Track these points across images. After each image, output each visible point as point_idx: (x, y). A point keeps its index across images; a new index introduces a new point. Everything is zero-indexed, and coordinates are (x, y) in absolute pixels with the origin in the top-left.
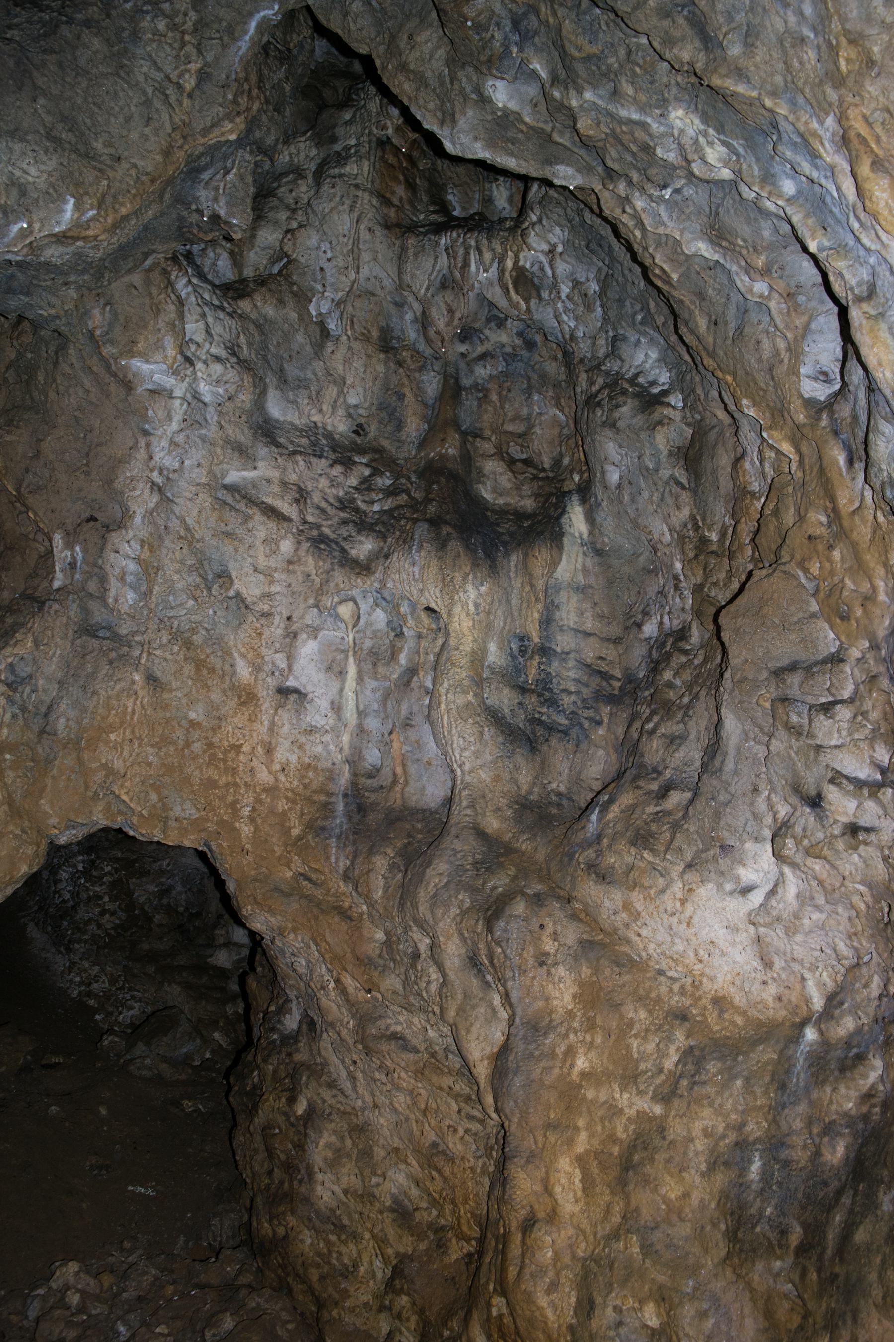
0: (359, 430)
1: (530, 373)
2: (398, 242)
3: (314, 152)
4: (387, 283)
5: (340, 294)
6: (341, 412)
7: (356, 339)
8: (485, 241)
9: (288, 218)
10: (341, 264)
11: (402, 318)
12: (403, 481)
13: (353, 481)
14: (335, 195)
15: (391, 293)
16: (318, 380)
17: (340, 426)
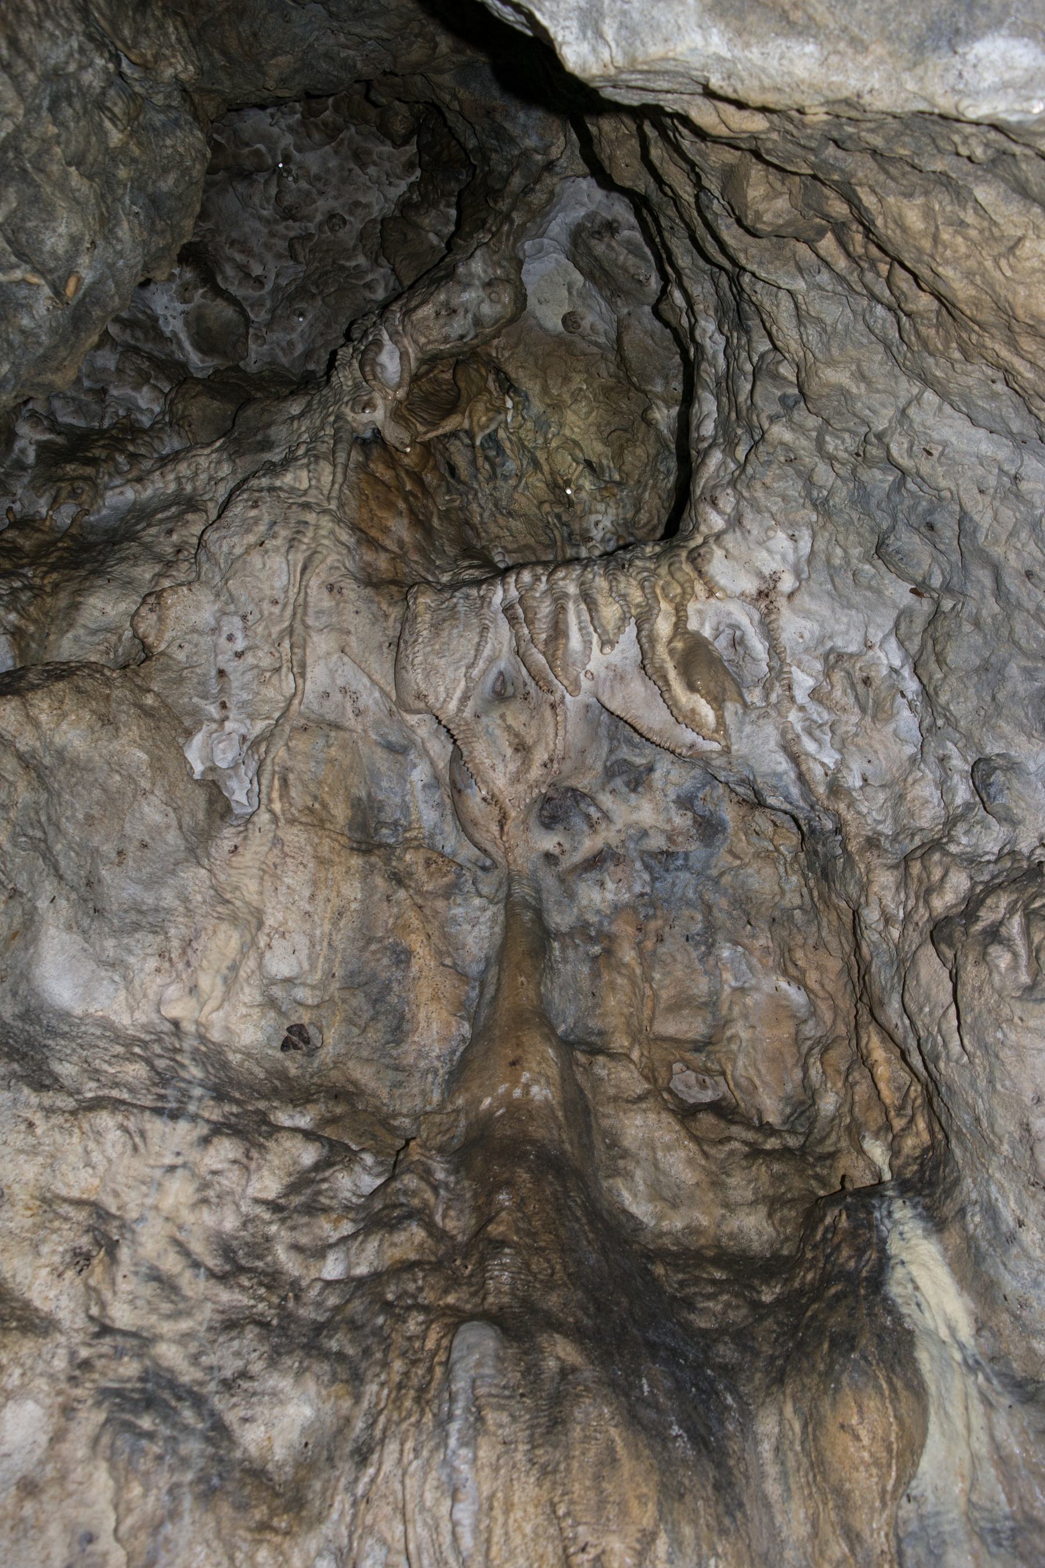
0: (296, 1039)
1: (709, 896)
2: (395, 612)
3: (226, 469)
4: (370, 698)
5: (260, 726)
6: (249, 994)
7: (292, 821)
8: (601, 583)
9: (159, 575)
10: (266, 662)
11: (403, 778)
12: (410, 1181)
13: (269, 1184)
14: (257, 521)
15: (377, 724)
16: (189, 912)
17: (245, 1030)
